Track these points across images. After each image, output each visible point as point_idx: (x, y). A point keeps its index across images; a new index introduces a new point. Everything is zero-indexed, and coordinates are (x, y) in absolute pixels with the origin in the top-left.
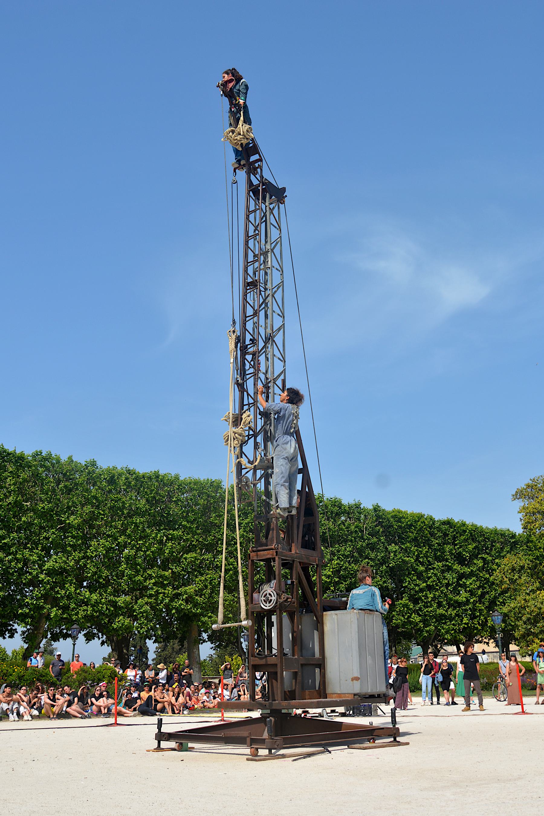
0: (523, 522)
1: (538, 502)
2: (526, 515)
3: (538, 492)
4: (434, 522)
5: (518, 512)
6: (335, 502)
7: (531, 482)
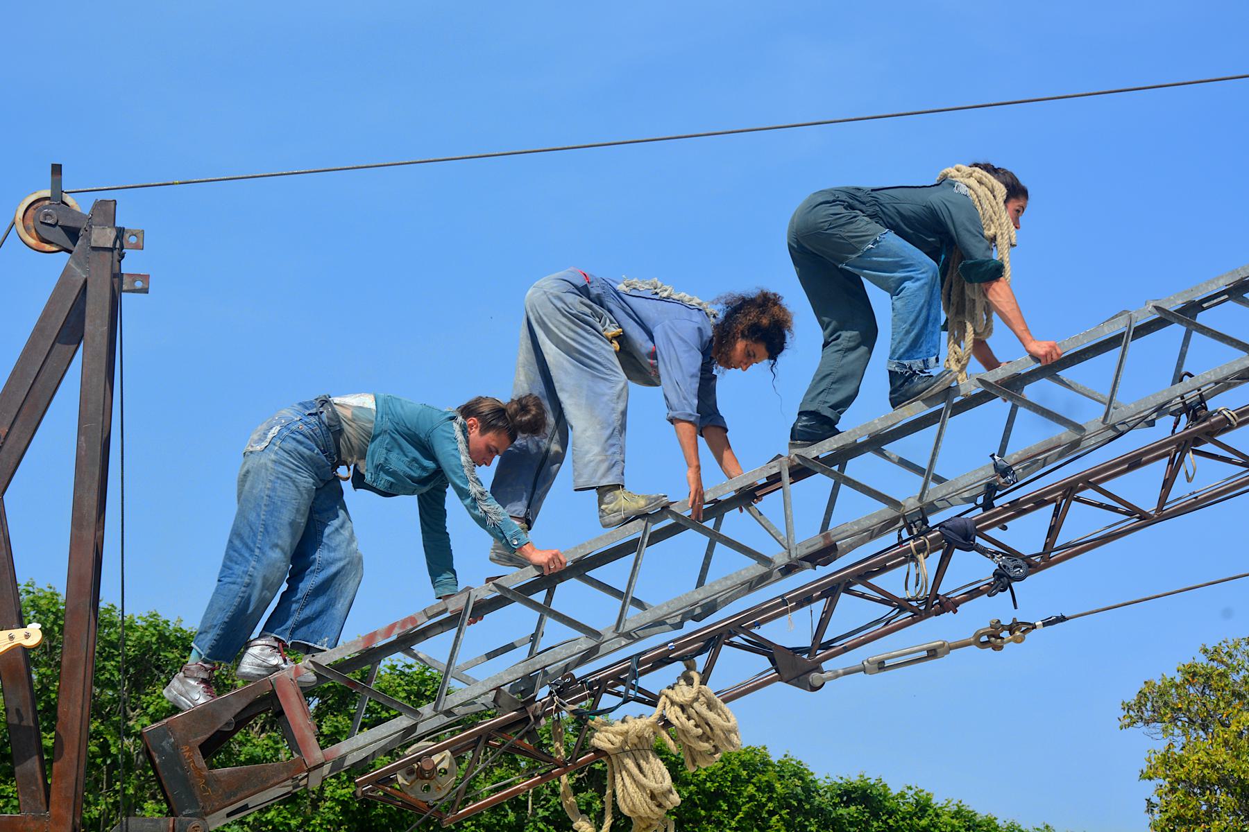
0: (1157, 816)
1: (1226, 743)
2: (1173, 790)
3: (1229, 704)
4: (809, 790)
5: (1145, 776)
6: (423, 682)
7: (1202, 660)
